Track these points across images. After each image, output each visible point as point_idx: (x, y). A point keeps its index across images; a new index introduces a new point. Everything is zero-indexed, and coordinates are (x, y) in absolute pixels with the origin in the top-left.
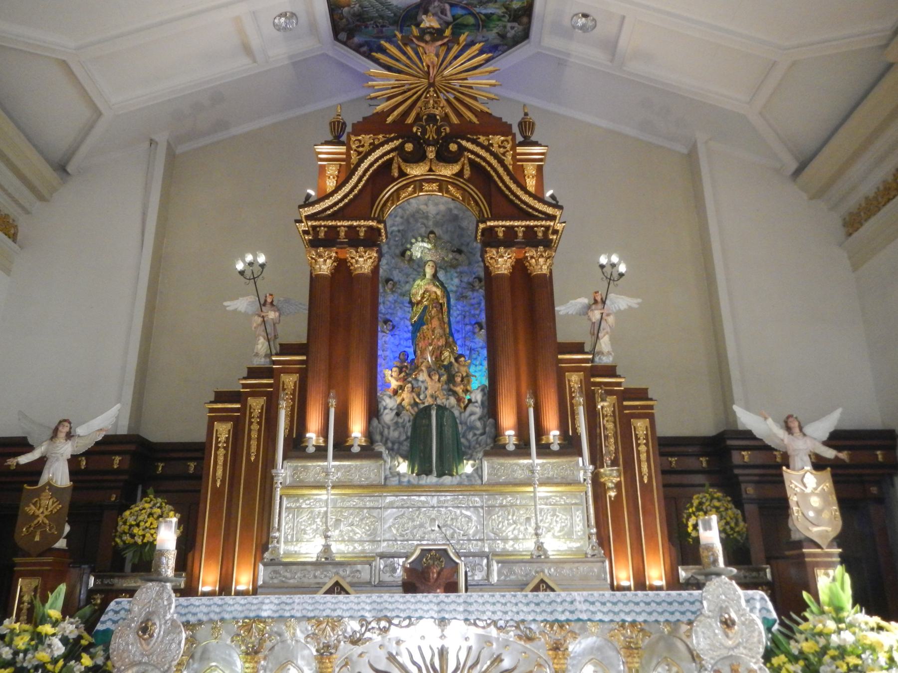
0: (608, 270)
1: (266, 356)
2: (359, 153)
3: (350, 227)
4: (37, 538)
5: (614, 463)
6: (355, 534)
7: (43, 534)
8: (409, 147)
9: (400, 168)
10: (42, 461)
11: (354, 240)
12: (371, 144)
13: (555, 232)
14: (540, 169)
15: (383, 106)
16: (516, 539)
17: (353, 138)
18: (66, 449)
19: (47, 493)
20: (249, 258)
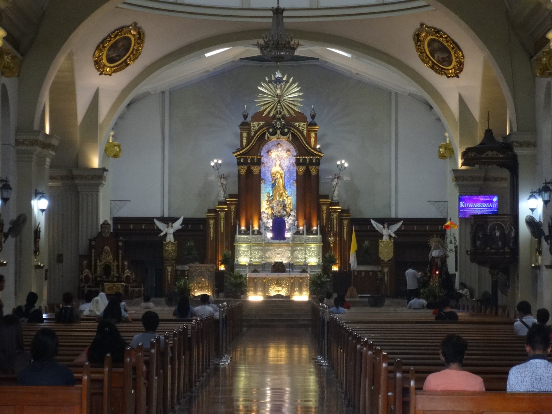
0: (340, 167)
1: (223, 197)
2: (254, 129)
3: (252, 158)
4: (170, 256)
5: (334, 235)
6: (256, 256)
7: (171, 255)
8: (271, 130)
9: (268, 136)
10: (166, 235)
11: (253, 163)
12: (258, 125)
13: (321, 156)
14: (316, 134)
15: (262, 108)
16: (301, 258)
17: (252, 123)
18: (171, 231)
19: (170, 244)
20: (215, 161)
